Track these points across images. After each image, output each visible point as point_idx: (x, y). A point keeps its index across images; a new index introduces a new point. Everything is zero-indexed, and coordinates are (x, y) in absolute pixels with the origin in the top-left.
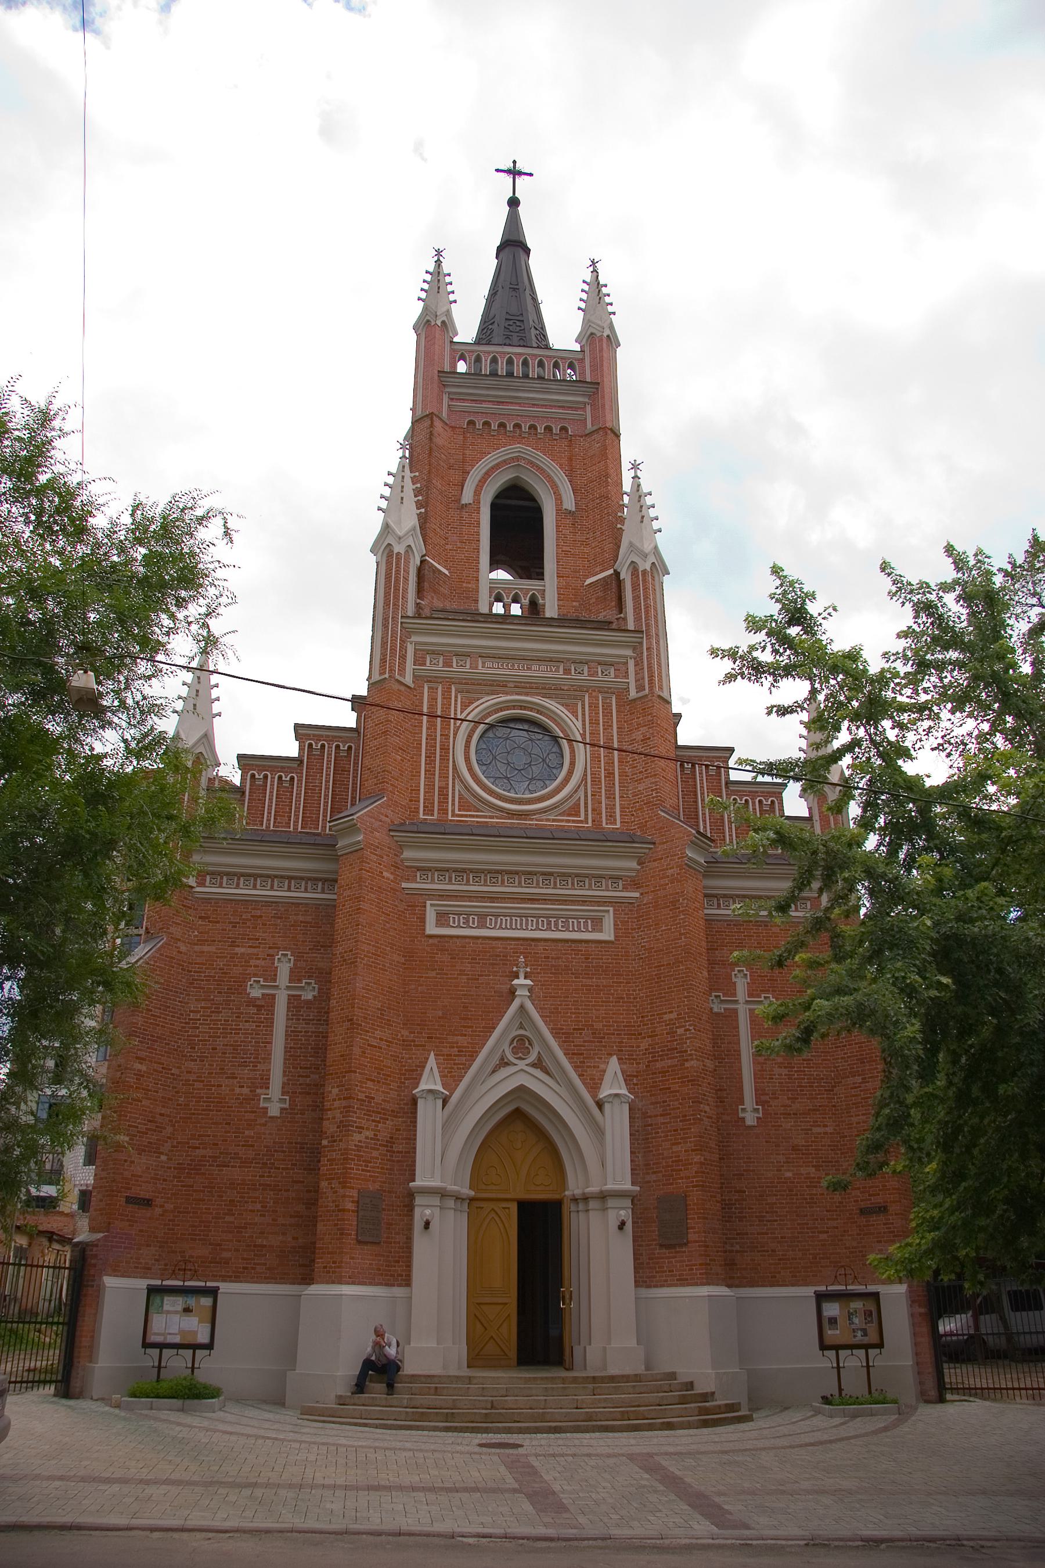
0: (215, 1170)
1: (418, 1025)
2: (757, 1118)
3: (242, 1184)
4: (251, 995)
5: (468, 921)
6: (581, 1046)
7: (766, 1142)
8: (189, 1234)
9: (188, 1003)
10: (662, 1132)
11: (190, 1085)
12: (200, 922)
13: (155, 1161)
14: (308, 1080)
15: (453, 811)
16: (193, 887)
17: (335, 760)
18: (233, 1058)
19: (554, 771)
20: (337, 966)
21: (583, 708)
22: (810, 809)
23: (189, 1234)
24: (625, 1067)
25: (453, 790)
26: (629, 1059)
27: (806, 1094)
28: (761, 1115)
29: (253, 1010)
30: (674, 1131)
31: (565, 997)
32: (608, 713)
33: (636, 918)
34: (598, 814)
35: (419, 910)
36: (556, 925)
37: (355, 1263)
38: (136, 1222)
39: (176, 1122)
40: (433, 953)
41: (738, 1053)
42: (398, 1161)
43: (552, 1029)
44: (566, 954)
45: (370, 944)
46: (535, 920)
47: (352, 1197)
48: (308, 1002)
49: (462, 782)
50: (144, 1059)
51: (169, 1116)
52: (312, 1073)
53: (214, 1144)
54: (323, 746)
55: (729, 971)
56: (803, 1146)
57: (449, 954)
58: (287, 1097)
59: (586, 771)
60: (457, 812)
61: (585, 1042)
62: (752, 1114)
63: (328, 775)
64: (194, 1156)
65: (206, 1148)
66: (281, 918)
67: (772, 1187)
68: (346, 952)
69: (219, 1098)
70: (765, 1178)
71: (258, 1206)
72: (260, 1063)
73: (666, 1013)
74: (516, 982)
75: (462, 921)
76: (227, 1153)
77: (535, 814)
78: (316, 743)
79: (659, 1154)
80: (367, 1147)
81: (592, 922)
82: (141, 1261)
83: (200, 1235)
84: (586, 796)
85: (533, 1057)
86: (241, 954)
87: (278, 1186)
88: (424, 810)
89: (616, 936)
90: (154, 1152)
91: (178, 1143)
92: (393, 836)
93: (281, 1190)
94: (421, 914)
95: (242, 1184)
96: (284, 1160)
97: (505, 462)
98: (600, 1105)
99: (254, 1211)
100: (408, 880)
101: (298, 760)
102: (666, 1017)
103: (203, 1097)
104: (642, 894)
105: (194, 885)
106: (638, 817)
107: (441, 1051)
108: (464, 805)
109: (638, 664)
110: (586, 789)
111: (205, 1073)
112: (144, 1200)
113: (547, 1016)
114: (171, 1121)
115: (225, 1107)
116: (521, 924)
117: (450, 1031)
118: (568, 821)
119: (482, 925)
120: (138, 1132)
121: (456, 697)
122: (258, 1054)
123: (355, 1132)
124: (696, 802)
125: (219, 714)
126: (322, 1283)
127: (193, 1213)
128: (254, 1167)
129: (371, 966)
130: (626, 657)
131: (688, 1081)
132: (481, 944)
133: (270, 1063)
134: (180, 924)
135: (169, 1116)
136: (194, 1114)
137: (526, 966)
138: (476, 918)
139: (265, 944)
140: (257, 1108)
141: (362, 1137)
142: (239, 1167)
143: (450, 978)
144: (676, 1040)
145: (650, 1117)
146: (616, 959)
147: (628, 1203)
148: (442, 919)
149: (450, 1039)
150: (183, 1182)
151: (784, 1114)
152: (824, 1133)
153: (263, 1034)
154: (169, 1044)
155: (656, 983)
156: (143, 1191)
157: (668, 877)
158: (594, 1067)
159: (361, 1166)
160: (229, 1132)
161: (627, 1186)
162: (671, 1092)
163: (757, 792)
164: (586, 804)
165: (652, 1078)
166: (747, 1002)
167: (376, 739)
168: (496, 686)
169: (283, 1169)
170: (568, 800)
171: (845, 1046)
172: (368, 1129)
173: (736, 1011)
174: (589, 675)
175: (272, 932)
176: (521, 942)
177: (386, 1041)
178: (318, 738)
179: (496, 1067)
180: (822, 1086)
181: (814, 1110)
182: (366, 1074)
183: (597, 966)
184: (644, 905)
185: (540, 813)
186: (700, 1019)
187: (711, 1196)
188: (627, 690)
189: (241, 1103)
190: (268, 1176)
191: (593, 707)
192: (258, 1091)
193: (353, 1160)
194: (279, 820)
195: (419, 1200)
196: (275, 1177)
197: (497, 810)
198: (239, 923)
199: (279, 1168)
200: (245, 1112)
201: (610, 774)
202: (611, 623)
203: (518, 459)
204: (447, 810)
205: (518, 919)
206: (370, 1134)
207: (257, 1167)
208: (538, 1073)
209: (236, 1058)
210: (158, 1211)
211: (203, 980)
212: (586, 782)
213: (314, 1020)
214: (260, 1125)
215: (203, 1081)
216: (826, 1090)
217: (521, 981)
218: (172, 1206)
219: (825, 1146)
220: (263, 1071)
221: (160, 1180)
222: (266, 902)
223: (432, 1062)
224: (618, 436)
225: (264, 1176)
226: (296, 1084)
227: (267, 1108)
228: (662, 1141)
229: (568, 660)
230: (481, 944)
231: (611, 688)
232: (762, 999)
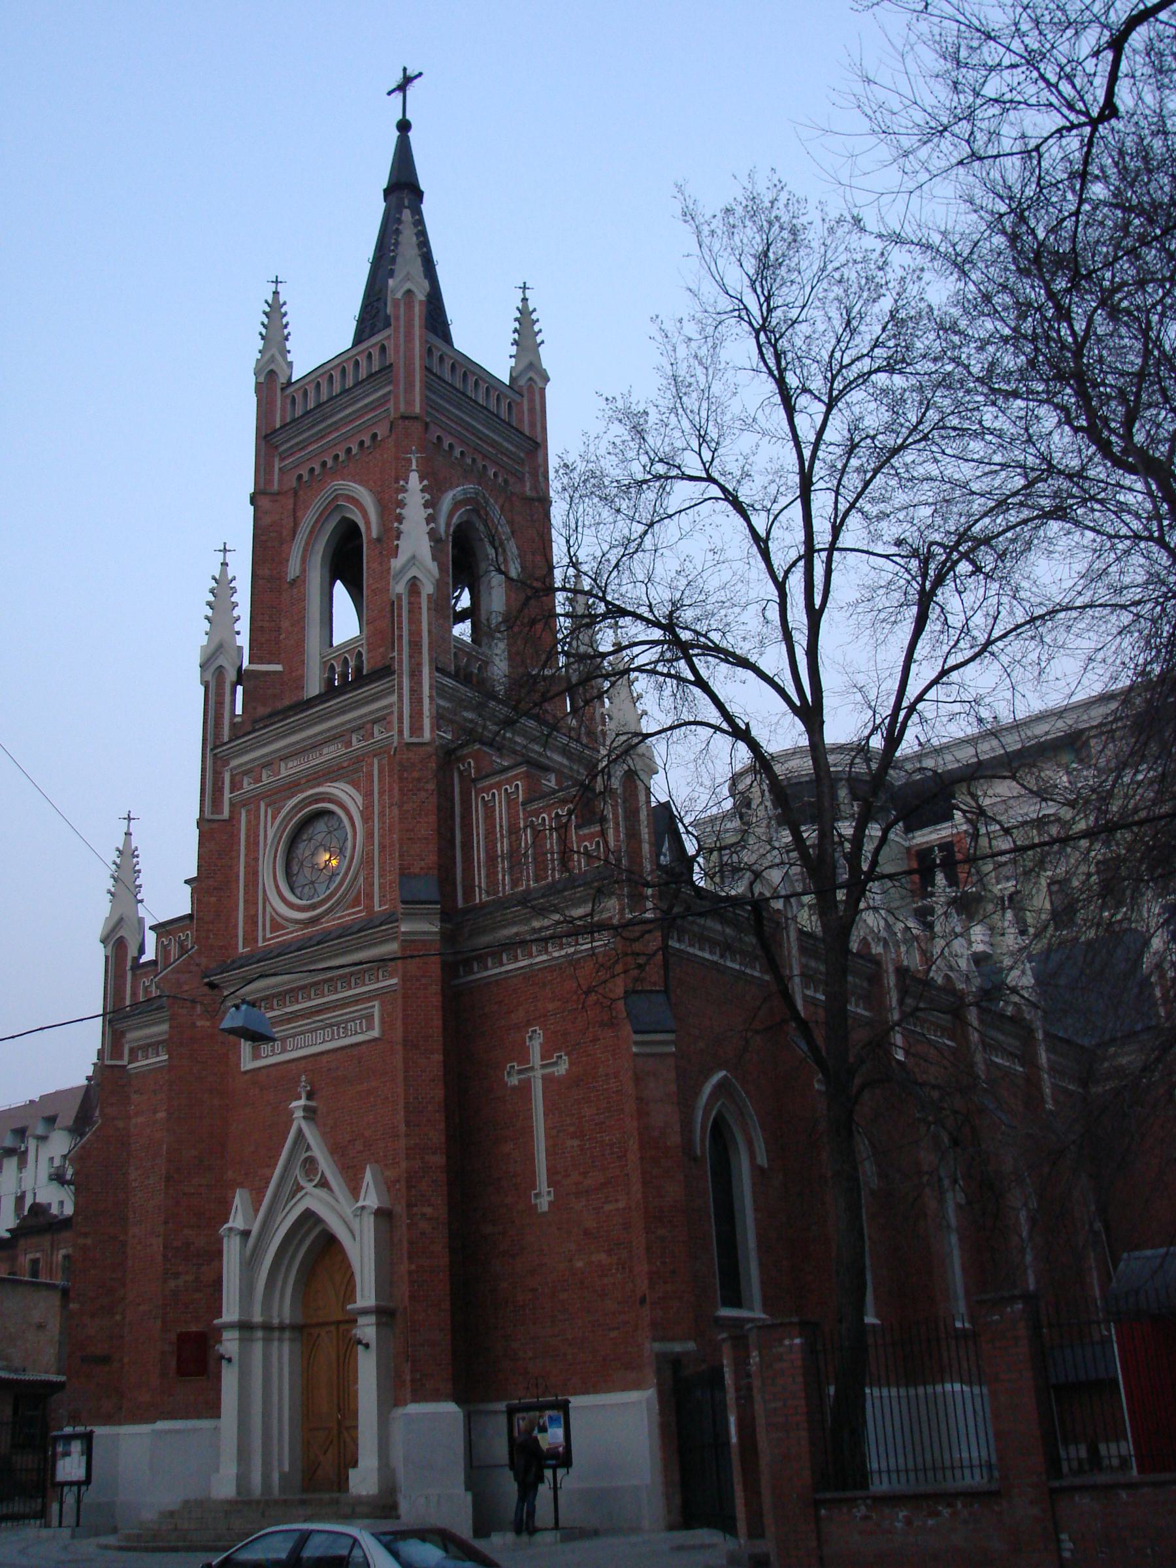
15: (264, 936)
41: (528, 1131)
60: (269, 936)
74: (294, 1104)
108: (276, 926)
118: (349, 915)
119: (284, 1050)
121: (266, 812)
141: (180, 1282)
147: (372, 1319)
166: (543, 1066)
168: (293, 786)
195: (227, 1335)
203: (336, 498)
206: (190, 1278)
208: (322, 1193)
223: (240, 1199)
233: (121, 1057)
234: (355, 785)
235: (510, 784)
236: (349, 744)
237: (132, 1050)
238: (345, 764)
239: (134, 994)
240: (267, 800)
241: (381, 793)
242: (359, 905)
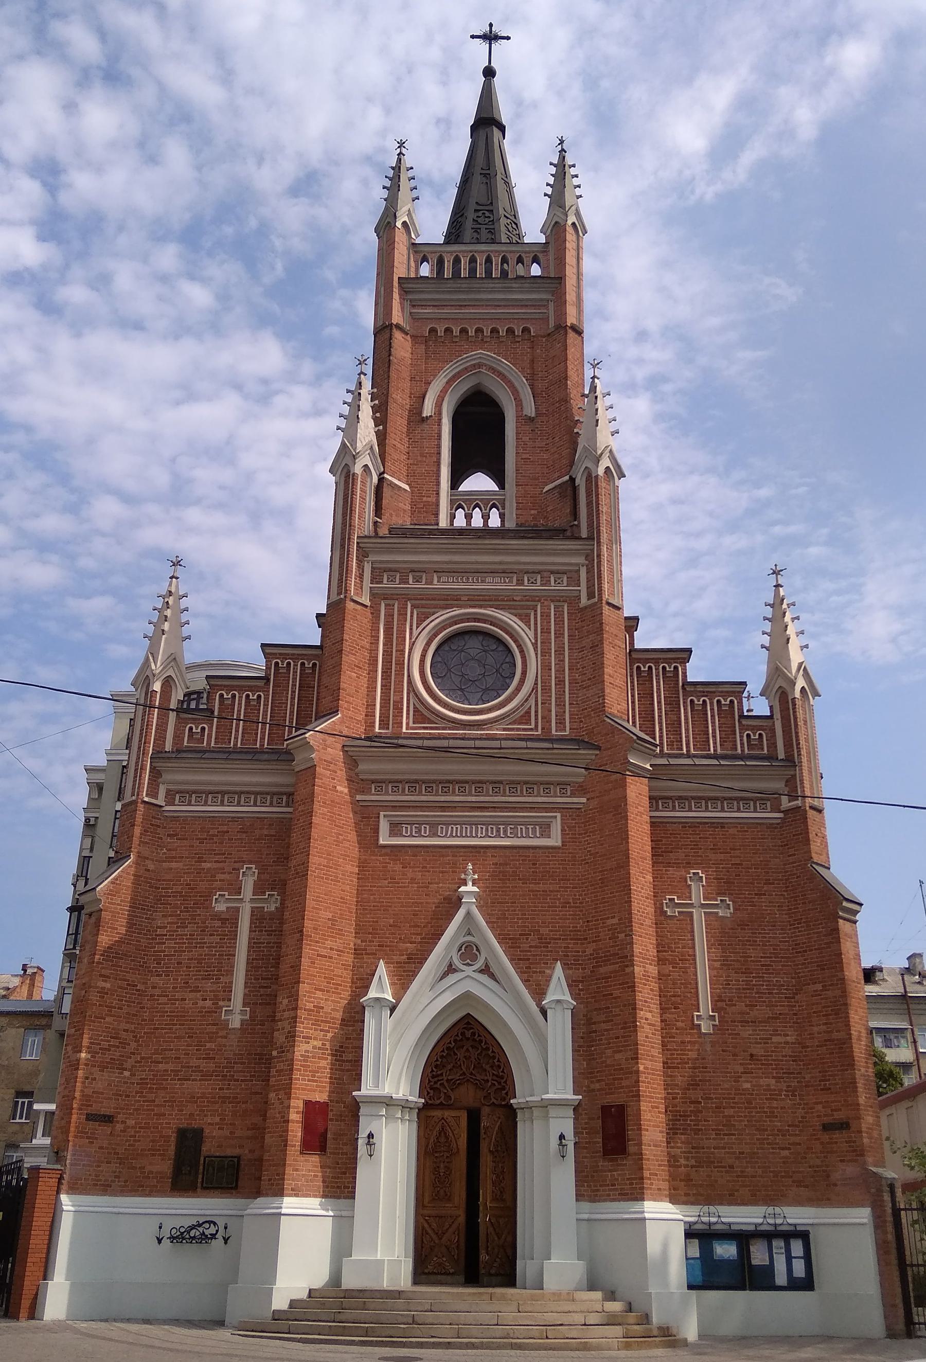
0: (176, 1084)
1: (369, 933)
2: (713, 1025)
3: (202, 1097)
4: (216, 909)
5: (420, 831)
6: (526, 951)
7: (723, 1051)
9: (155, 920)
10: (606, 1039)
12: (169, 840)
13: (116, 1077)
15: (407, 724)
16: (162, 807)
17: (300, 677)
19: (508, 681)
20: (290, 879)
21: (536, 618)
22: (771, 707)
24: (571, 972)
25: (408, 703)
26: (575, 965)
27: (765, 1002)
28: (717, 1023)
29: (218, 924)
30: (617, 1038)
31: (512, 903)
32: (559, 621)
33: (582, 823)
34: (547, 722)
35: (374, 821)
36: (505, 831)
37: (299, 1175)
38: (96, 1138)
39: (140, 1037)
40: (386, 863)
42: (348, 1070)
43: (499, 935)
44: (513, 860)
45: (322, 857)
46: (484, 827)
47: (298, 1107)
48: (270, 913)
49: (417, 696)
50: (108, 977)
51: (133, 1032)
53: (176, 1058)
54: (289, 664)
55: (683, 873)
56: (762, 1056)
57: (402, 863)
58: (248, 1009)
59: (536, 680)
61: (530, 947)
62: (708, 1021)
63: (293, 692)
64: (157, 1071)
65: (167, 1063)
66: (246, 832)
67: (729, 1098)
68: (299, 865)
69: (183, 1012)
70: (722, 1089)
71: (217, 1119)
72: (223, 975)
73: (608, 918)
74: (462, 889)
75: (414, 830)
76: (188, 1067)
77: (486, 725)
78: (282, 662)
79: (603, 1062)
80: (314, 1057)
81: (541, 828)
82: (100, 1178)
83: (159, 1150)
84: (536, 705)
85: (479, 964)
86: (207, 869)
88: (380, 724)
89: (563, 842)
90: (117, 1068)
91: (142, 1058)
92: (347, 751)
94: (374, 825)
95: (202, 1097)
97: (466, 370)
98: (544, 1013)
99: (212, 1124)
100: (363, 792)
101: (266, 679)
102: (610, 922)
104: (588, 799)
105: (163, 804)
106: (585, 723)
107: (392, 959)
109: (590, 571)
110: (537, 698)
111: (169, 988)
112: (105, 1116)
113: (494, 922)
114: (135, 1037)
116: (471, 832)
117: (400, 939)
118: (518, 729)
119: (434, 834)
120: (100, 1049)
123: (302, 1042)
124: (653, 704)
125: (189, 637)
126: (267, 1195)
129: (322, 878)
130: (578, 565)
131: (629, 987)
132: (432, 852)
134: (148, 843)
135: (133, 1032)
136: (157, 1029)
137: (474, 873)
138: (428, 827)
139: (230, 858)
141: (309, 1047)
142: (200, 1080)
143: (401, 887)
144: (618, 945)
145: (594, 1023)
146: (563, 864)
148: (395, 829)
149: (402, 946)
150: (145, 1097)
151: (742, 1022)
152: (785, 1043)
153: (227, 947)
154: (134, 961)
155: (601, 887)
156: (105, 1109)
157: (612, 782)
158: (540, 972)
159: (308, 1076)
161: (570, 1096)
162: (615, 998)
163: (714, 692)
164: (536, 712)
165: (596, 984)
166: (703, 906)
167: (332, 658)
168: (449, 600)
170: (518, 709)
171: (805, 951)
172: (315, 1039)
173: (691, 914)
174: (542, 585)
175: (238, 847)
176: (471, 849)
177: (337, 950)
178: (284, 657)
179: (444, 974)
180: (782, 994)
181: (773, 1018)
182: (314, 984)
183: (544, 872)
184: (591, 810)
185: (492, 723)
186: (642, 924)
187: (653, 1107)
188: (579, 598)
189: (204, 1016)
190: (228, 1089)
191: (546, 616)
192: (221, 1003)
193: (299, 1070)
194: (246, 738)
197: (449, 721)
198: (206, 839)
201: (560, 682)
202: (565, 530)
204: (402, 723)
205: (468, 827)
206: (318, 1044)
207: (217, 1080)
208: (484, 978)
209: (200, 971)
210: (119, 1127)
211: (170, 896)
212: (537, 691)
213: (275, 931)
214: (222, 1037)
215: (167, 996)
216: (786, 998)
217: (470, 887)
219: (786, 1056)
221: (121, 1095)
222: (233, 818)
223: (382, 969)
224: (579, 332)
225: (223, 1089)
227: (228, 1020)
228: (606, 1049)
229: (521, 571)
230: (432, 852)
231: (563, 596)
232: (719, 902)
233: (155, 796)
234: (525, 619)
235: (670, 664)
236: (520, 582)
237: (168, 792)
238: (515, 598)
239: (178, 737)
240: (414, 602)
241: (559, 635)
242: (526, 724)
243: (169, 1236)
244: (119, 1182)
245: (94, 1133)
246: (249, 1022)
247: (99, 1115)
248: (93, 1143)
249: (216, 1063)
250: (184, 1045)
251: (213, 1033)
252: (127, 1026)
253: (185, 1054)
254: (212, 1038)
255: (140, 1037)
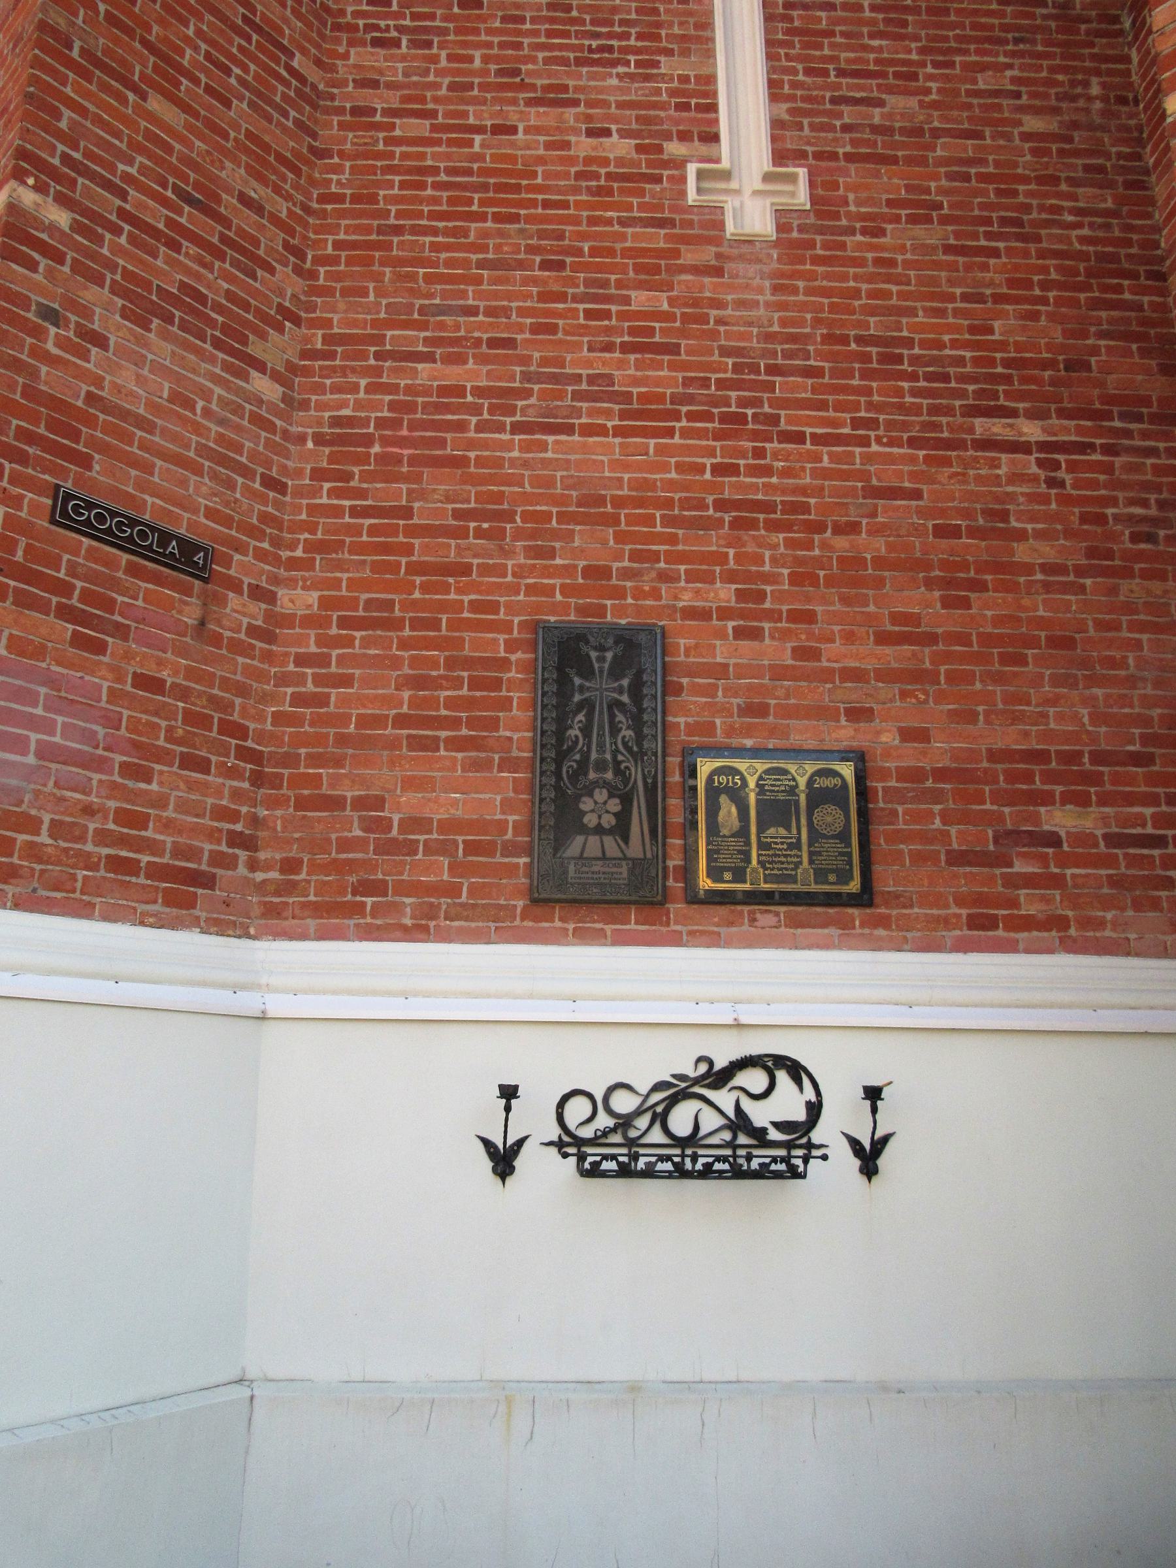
0: (508, 446)
8: (401, 721)
11: (377, 127)
14: (877, 116)
18: (550, 34)
23: (401, 721)
38: (121, 632)
52: (890, 90)
53: (493, 343)
64: (409, 390)
71: (724, 593)
72: (669, 52)
76: (554, 378)
83: (455, 723)
87: (805, 508)
93: (820, 528)
95: (640, 503)
96: (822, 405)
99: (703, 615)
103: (435, 171)
111: (436, 86)
112: (165, 537)
115: (533, 203)
122: (659, 25)
127: (416, 624)
128: (685, 433)
133: (710, 54)
136: (398, 230)
140: (674, 209)
142: (619, 432)
150: (361, 494)
160: (562, 297)
169: (817, 439)
192: (674, 148)
196: (786, 473)
199: (799, 438)
200: (622, 222)
209: (565, 34)
214: (697, 270)
215: (433, 114)
218: (313, 597)
220: (684, 79)
225: (733, 470)
226: (831, 128)
243: (554, 1133)
244: (253, 866)
245: (109, 606)
246: (812, 220)
247: (133, 523)
248: (100, 648)
249: (685, 366)
250: (528, 296)
251: (660, 253)
252: (256, 191)
253: (536, 329)
254: (656, 270)
255: (318, 261)
